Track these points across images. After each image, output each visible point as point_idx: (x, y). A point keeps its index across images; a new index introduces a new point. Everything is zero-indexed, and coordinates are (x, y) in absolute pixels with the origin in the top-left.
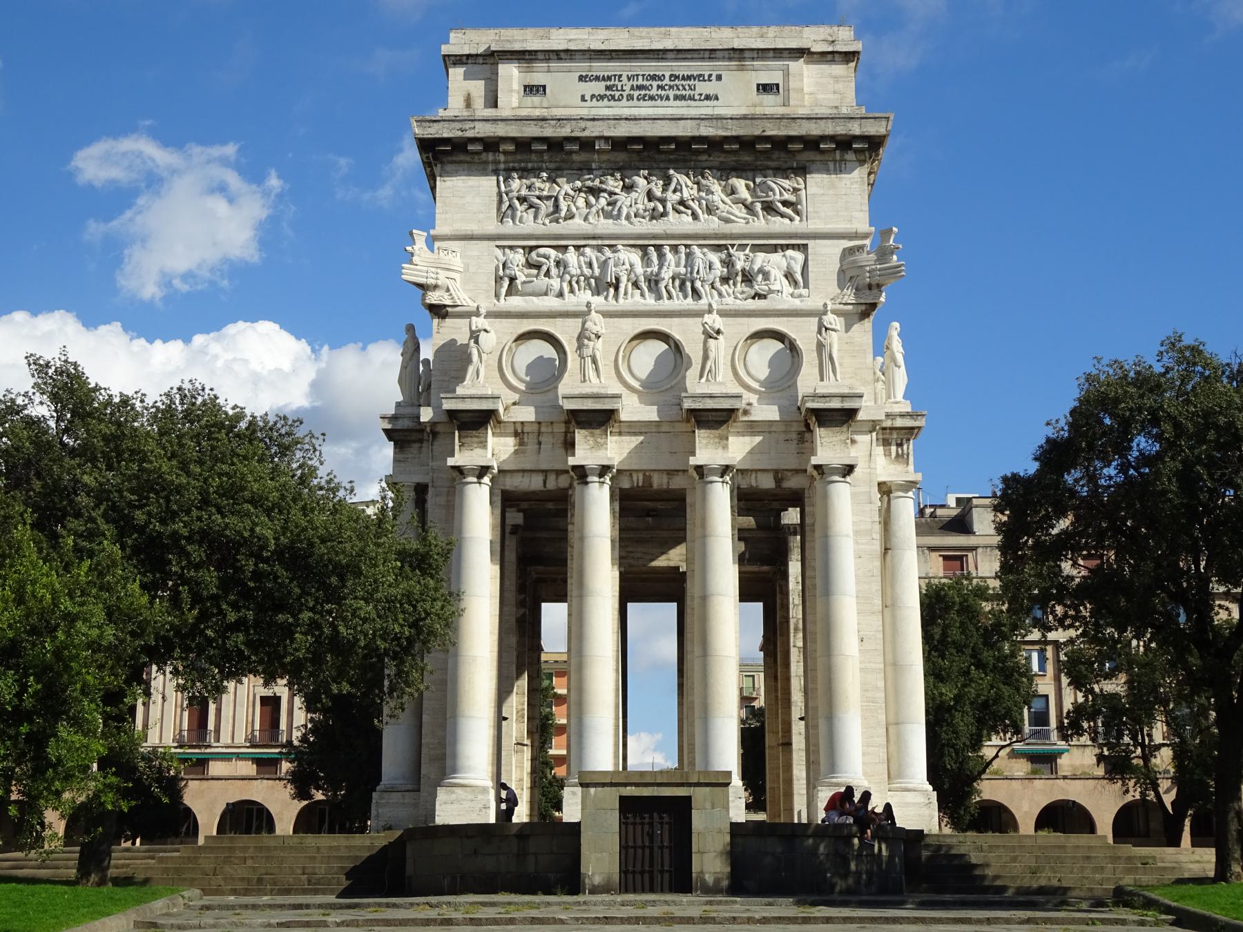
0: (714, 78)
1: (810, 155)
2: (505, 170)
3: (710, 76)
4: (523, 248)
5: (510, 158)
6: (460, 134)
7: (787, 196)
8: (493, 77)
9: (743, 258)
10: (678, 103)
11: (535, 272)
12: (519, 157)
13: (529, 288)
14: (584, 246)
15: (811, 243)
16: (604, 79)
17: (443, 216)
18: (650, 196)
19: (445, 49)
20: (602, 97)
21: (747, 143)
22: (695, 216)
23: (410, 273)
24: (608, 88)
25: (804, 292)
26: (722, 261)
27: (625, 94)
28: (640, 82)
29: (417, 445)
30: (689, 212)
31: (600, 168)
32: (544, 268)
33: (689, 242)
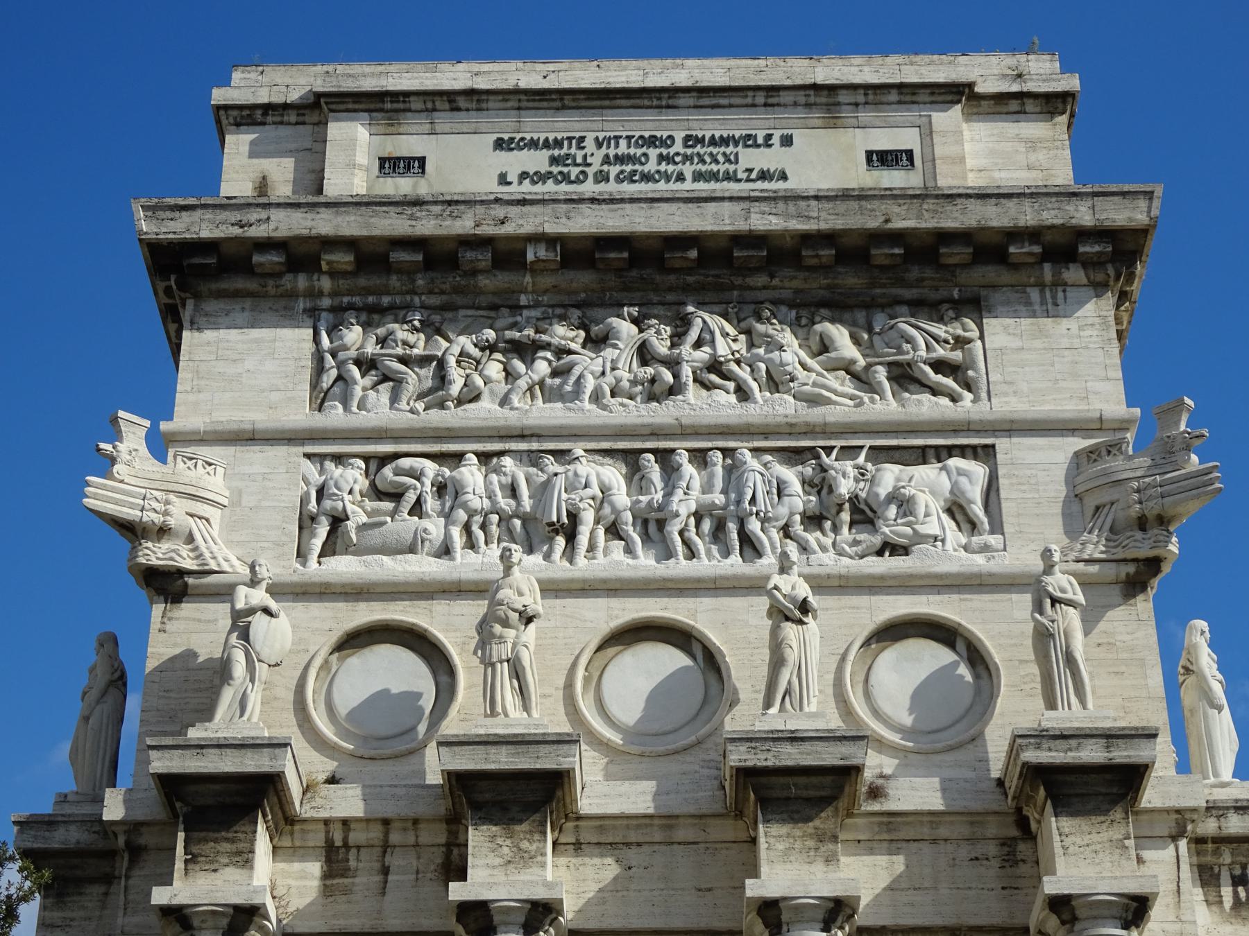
0: (776, 140)
1: (988, 273)
2: (332, 310)
3: (769, 137)
4: (366, 458)
5: (343, 284)
6: (236, 231)
7: (940, 352)
8: (317, 147)
9: (852, 472)
11: (388, 505)
12: (362, 281)
13: (375, 537)
14: (501, 453)
15: (1002, 445)
16: (547, 145)
17: (191, 397)
18: (644, 354)
19: (219, 96)
22: (743, 394)
23: (102, 496)
24: (554, 161)
25: (994, 540)
26: (806, 483)
27: (591, 171)
28: (623, 148)
29: (97, 890)
30: (731, 385)
31: (536, 305)
32: (411, 497)
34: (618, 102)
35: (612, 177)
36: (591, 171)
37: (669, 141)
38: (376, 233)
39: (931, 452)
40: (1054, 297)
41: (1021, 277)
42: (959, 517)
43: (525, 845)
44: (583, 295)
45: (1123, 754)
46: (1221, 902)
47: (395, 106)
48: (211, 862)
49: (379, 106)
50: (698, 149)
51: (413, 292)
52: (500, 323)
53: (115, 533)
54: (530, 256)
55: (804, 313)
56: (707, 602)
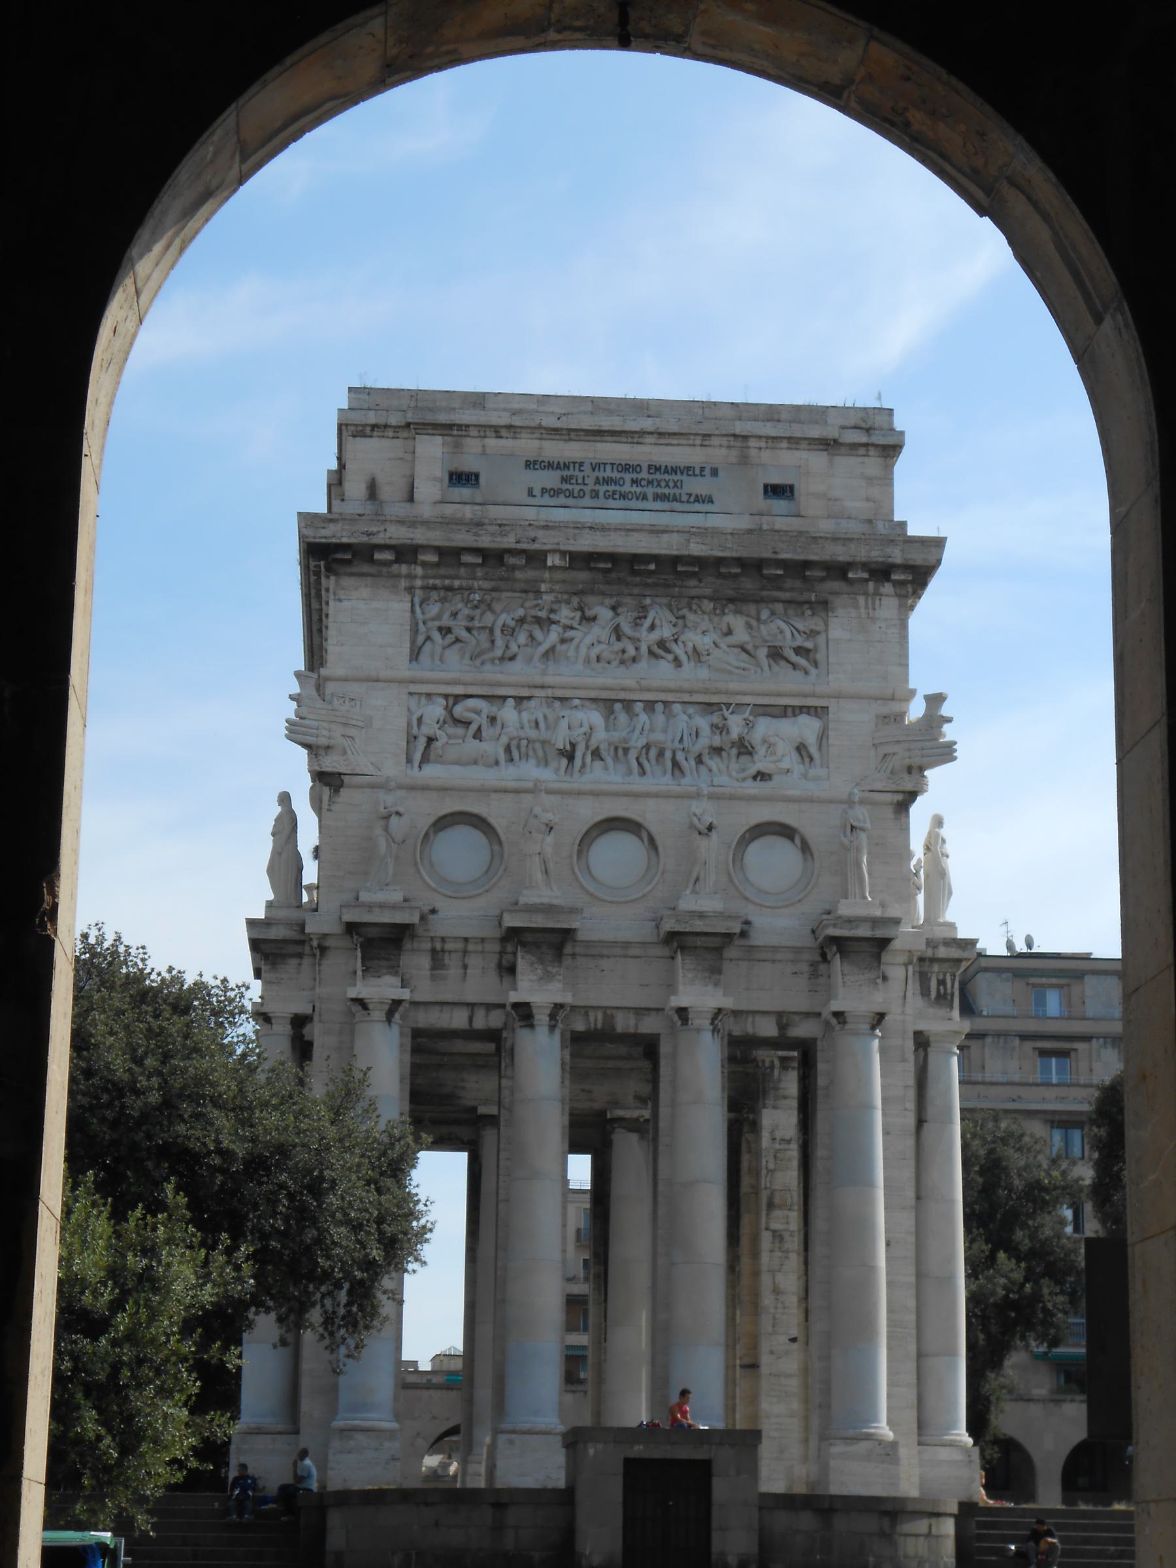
0: (707, 472)
1: (836, 585)
2: (424, 588)
3: (702, 469)
4: (446, 696)
6: (365, 539)
7: (800, 641)
10: (659, 505)
11: (460, 731)
12: (442, 571)
14: (529, 698)
16: (558, 467)
18: (618, 633)
20: (555, 493)
21: (753, 566)
22: (677, 662)
24: (564, 480)
25: (822, 772)
26: (714, 727)
28: (609, 473)
29: (294, 962)
30: (670, 657)
31: (552, 591)
32: (473, 727)
33: (670, 697)
35: (601, 494)
37: (636, 468)
39: (790, 711)
40: (873, 604)
42: (804, 753)
43: (550, 969)
44: (581, 586)
50: (658, 476)
51: (474, 579)
52: (528, 604)
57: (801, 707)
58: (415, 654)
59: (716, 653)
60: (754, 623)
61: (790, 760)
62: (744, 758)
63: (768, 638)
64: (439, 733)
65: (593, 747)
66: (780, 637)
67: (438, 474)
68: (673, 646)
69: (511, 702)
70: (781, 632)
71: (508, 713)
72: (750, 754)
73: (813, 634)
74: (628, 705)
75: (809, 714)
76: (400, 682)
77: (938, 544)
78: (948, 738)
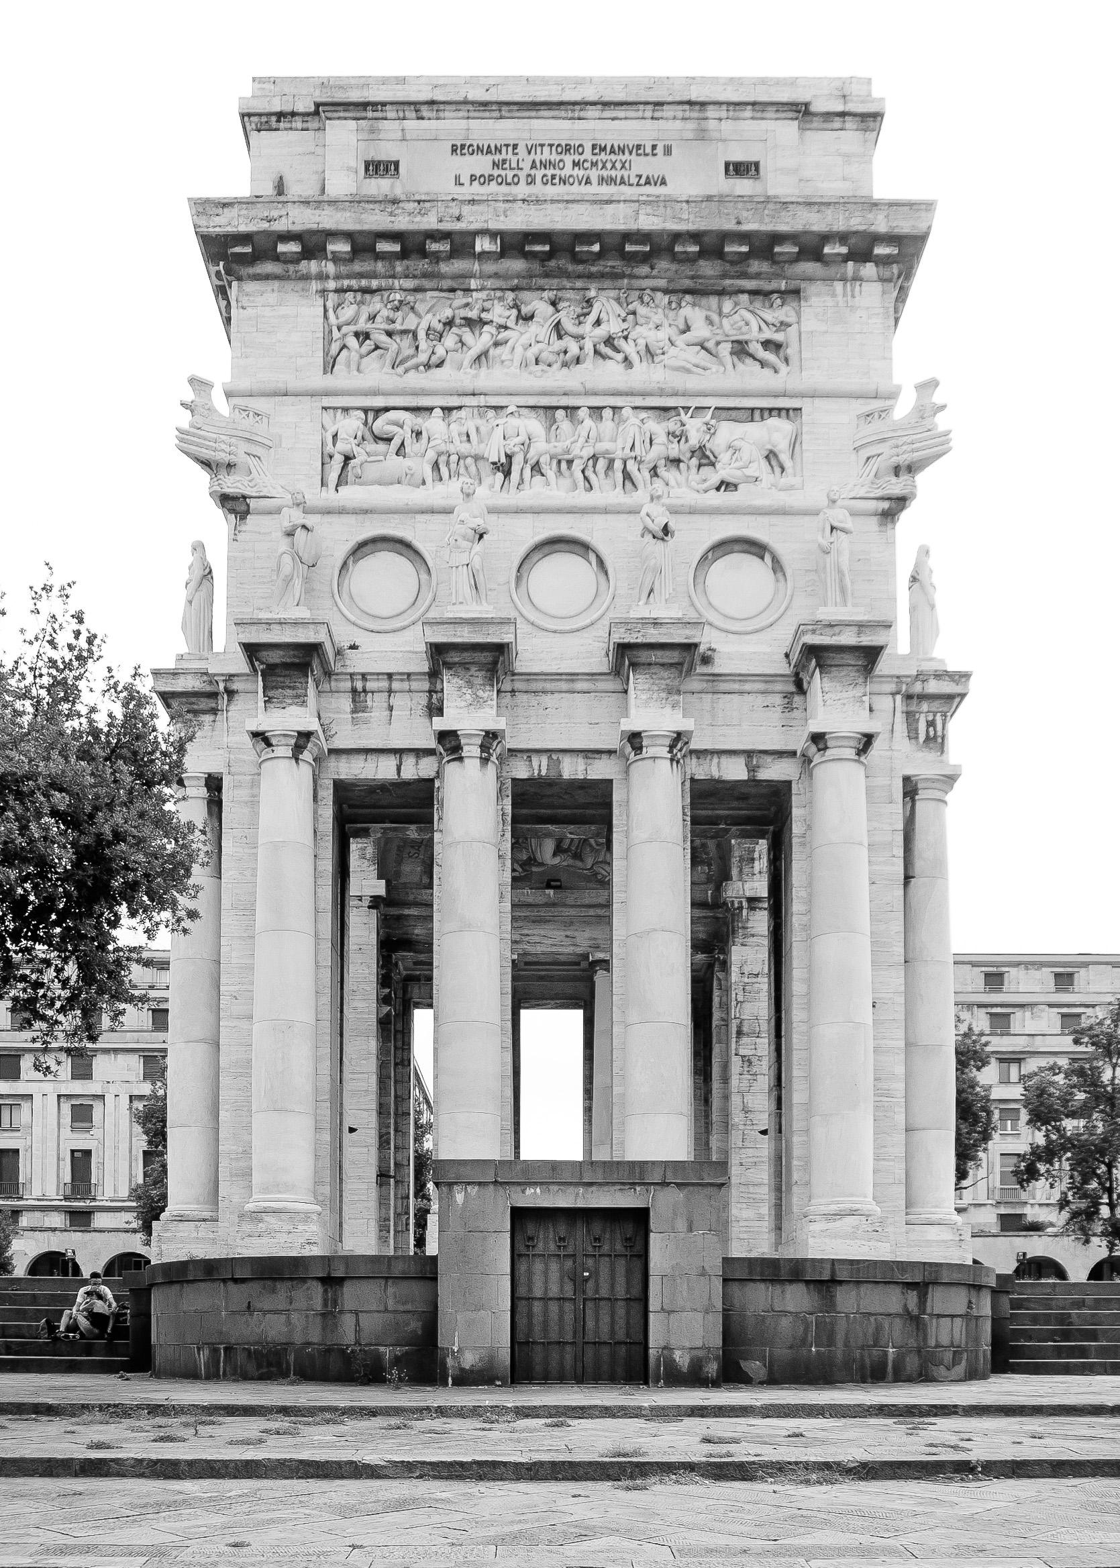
0: (660, 150)
1: (809, 267)
2: (337, 291)
3: (654, 147)
4: (366, 411)
5: (343, 269)
6: (265, 226)
7: (768, 334)
10: (606, 191)
11: (382, 447)
12: (357, 267)
14: (460, 408)
16: (489, 152)
21: (711, 245)
28: (546, 155)
30: (620, 357)
32: (396, 442)
33: (617, 401)
34: (542, 113)
35: (538, 179)
36: (522, 175)
38: (366, 227)
39: (757, 414)
40: (852, 291)
41: (833, 271)
42: (774, 463)
44: (516, 281)
45: (867, 640)
46: (917, 738)
47: (376, 114)
48: (281, 702)
49: (363, 114)
50: (603, 157)
51: (393, 277)
53: (197, 467)
54: (478, 249)
55: (674, 298)
56: (599, 519)
57: (771, 410)
58: (330, 365)
59: (672, 351)
60: (715, 317)
61: (760, 468)
62: (704, 470)
63: (730, 333)
64: (356, 450)
65: (533, 461)
66: (745, 329)
67: (353, 164)
68: (620, 343)
69: (438, 412)
70: (747, 324)
71: (434, 424)
72: (713, 465)
73: (784, 325)
74: (571, 410)
75: (779, 416)
76: (312, 394)
77: (928, 206)
78: (941, 428)
